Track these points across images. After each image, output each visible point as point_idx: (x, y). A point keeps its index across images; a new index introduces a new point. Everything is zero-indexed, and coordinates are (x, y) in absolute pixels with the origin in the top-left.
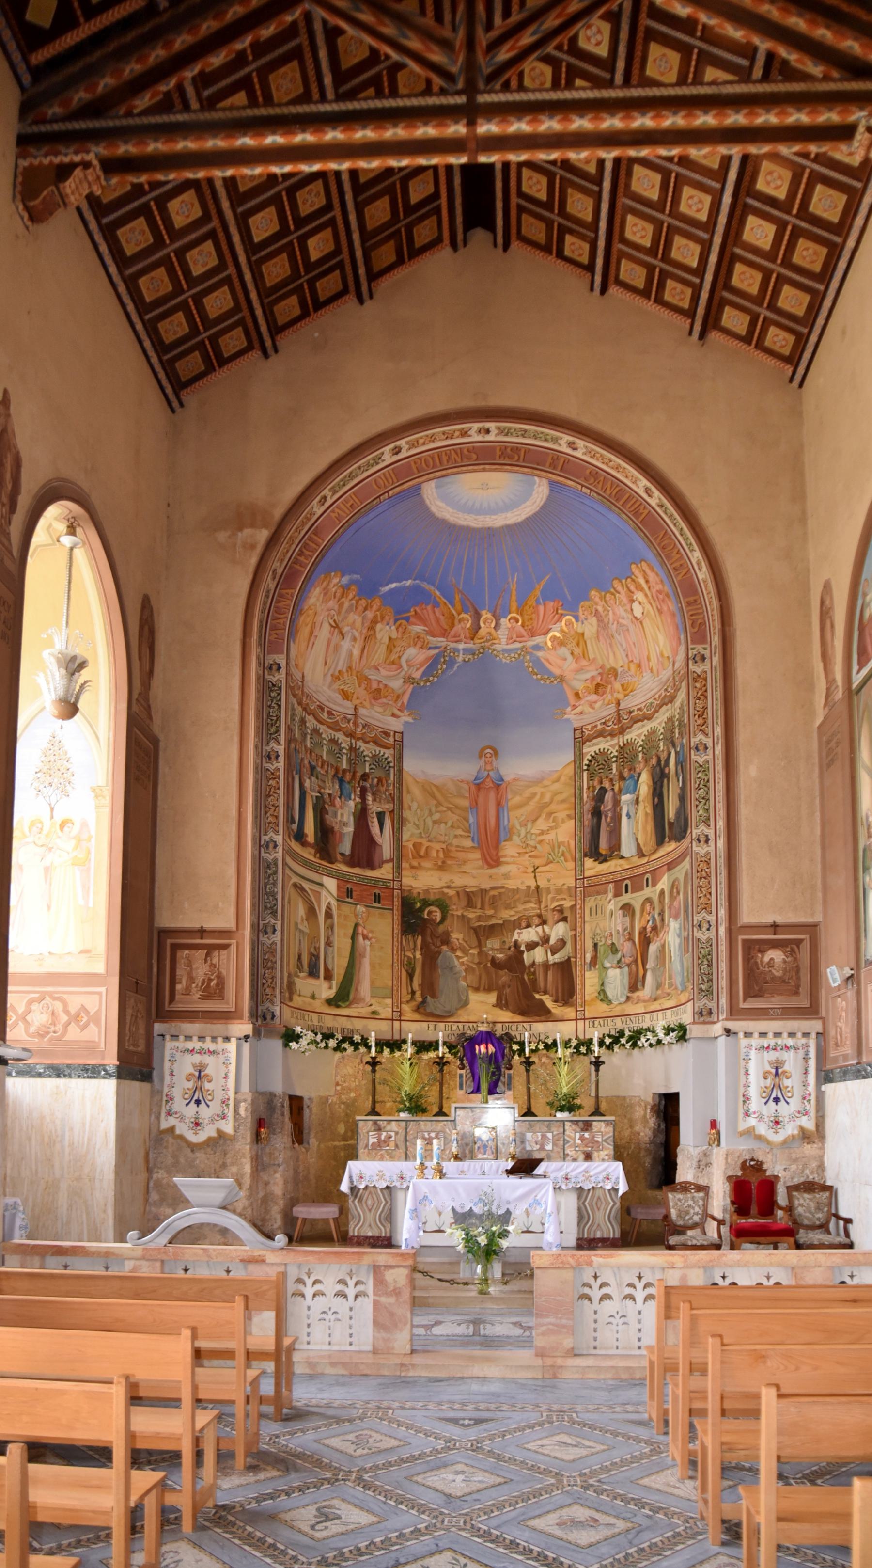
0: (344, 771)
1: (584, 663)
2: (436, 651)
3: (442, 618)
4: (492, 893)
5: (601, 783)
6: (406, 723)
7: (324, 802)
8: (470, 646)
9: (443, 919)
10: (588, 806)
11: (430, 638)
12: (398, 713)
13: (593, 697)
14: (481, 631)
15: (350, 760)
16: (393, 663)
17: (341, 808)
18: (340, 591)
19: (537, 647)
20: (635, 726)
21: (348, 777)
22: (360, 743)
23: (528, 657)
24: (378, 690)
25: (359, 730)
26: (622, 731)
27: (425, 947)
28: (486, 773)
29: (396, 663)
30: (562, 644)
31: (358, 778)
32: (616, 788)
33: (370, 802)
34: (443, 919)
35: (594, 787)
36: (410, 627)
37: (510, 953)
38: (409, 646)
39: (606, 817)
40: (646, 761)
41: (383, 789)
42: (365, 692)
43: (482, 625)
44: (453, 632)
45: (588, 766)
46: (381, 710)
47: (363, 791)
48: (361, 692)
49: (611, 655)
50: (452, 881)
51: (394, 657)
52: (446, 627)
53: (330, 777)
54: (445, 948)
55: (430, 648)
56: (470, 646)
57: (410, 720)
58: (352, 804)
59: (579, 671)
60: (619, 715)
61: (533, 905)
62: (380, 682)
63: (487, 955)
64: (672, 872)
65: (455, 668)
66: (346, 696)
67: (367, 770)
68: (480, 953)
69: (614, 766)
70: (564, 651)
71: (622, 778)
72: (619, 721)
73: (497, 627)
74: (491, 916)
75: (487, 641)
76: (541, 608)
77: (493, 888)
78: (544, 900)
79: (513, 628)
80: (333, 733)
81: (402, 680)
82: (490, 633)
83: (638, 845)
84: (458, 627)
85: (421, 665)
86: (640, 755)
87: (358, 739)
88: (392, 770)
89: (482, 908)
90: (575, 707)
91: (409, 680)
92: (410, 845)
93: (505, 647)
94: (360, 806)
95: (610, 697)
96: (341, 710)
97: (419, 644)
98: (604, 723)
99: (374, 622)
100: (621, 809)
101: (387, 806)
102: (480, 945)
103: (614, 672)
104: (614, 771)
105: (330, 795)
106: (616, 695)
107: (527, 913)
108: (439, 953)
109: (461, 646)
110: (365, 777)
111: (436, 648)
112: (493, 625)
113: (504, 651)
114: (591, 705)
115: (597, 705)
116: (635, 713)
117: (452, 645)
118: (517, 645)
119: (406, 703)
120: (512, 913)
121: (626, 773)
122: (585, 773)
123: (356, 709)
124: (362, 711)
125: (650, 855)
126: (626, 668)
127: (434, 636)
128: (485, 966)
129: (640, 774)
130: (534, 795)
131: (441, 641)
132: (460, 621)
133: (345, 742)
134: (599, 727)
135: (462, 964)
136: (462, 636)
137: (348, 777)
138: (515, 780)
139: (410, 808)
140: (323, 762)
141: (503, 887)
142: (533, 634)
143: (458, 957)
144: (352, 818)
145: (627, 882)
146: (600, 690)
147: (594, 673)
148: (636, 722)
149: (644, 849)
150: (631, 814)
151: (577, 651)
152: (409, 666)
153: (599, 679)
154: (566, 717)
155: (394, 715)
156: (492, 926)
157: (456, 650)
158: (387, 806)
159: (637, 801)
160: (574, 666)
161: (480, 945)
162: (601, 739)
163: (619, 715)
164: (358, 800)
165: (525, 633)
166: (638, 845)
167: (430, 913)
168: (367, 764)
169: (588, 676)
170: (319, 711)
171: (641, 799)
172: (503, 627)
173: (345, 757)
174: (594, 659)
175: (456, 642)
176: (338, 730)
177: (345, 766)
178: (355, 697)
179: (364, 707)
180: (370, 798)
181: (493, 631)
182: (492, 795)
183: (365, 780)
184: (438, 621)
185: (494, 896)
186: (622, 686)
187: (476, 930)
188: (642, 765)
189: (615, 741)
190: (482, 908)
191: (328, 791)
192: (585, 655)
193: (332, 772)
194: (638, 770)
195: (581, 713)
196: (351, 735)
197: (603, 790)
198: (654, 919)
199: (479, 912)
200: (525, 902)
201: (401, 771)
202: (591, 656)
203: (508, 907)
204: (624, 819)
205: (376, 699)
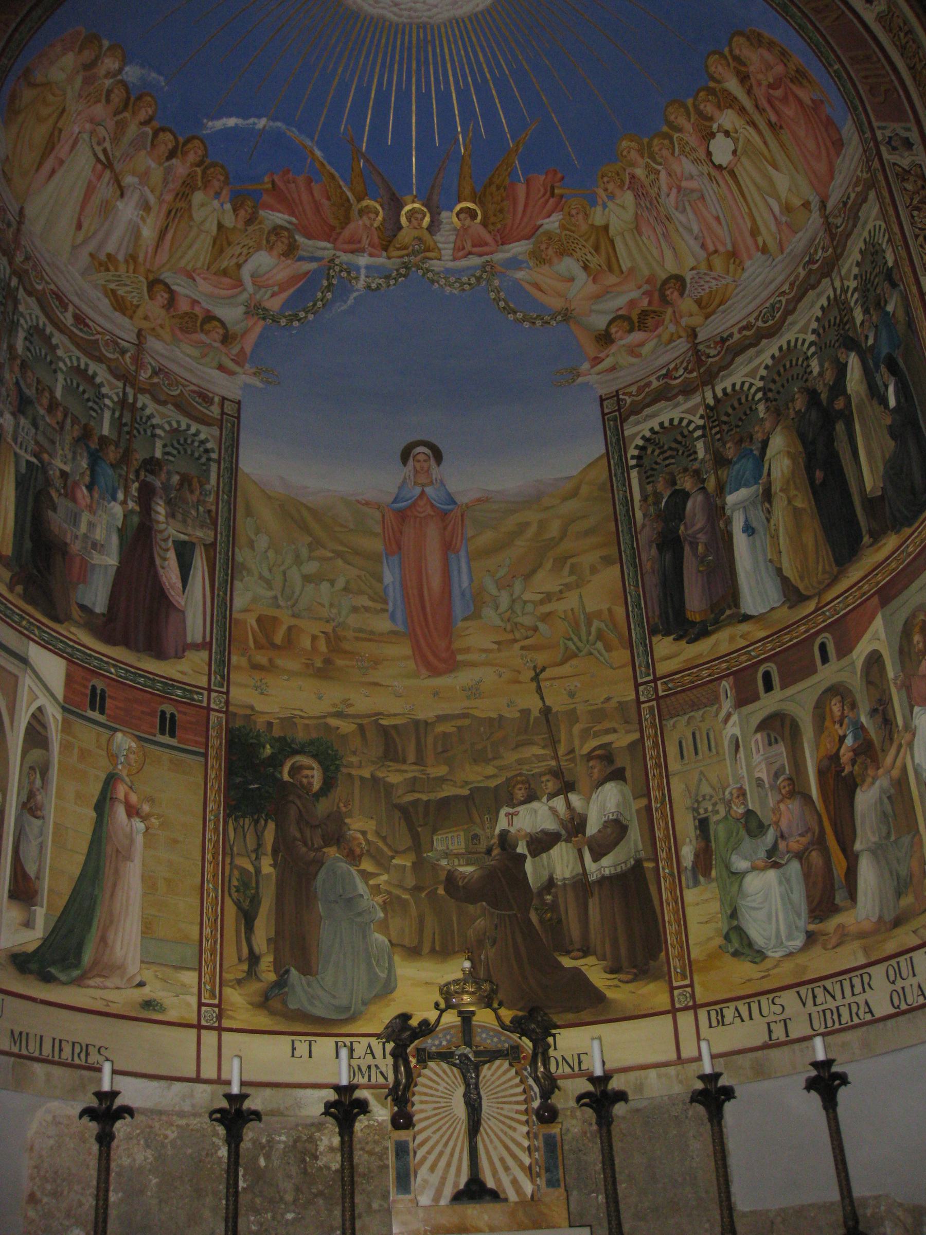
0: (103, 440)
1: (612, 279)
2: (313, 266)
3: (324, 201)
4: (440, 728)
5: (674, 483)
6: (246, 386)
7: (48, 482)
8: (381, 260)
9: (328, 784)
10: (643, 538)
11: (300, 239)
12: (231, 365)
13: (637, 336)
14: (403, 233)
15: (118, 424)
16: (225, 273)
17: (91, 509)
18: (117, 97)
19: (515, 263)
20: (738, 360)
21: (112, 454)
22: (143, 399)
23: (496, 283)
24: (192, 316)
25: (144, 375)
26: (709, 378)
27: (283, 848)
28: (418, 490)
29: (232, 275)
30: (564, 252)
31: (135, 464)
32: (711, 485)
33: (162, 518)
34: (328, 784)
35: (658, 496)
36: (262, 213)
37: (490, 862)
38: (259, 248)
39: (694, 545)
40: (777, 414)
41: (192, 498)
42: (163, 312)
43: (403, 220)
44: (346, 233)
45: (639, 458)
46: (195, 353)
47: (146, 495)
48: (154, 308)
49: (668, 254)
50: (347, 702)
51: (226, 262)
52: (333, 222)
53: (68, 439)
54: (332, 852)
55: (301, 259)
56: (381, 260)
57: (256, 382)
58: (117, 510)
59: (598, 297)
60: (697, 353)
61: (537, 750)
62: (195, 302)
63: (435, 867)
64: (895, 604)
65: (351, 301)
66: (120, 305)
67: (158, 454)
68: (418, 865)
69: (700, 446)
70: (570, 265)
71: (720, 461)
72: (700, 363)
73: (433, 228)
74: (442, 780)
75: (415, 253)
76: (521, 190)
77: (441, 719)
78: (563, 736)
79: (465, 229)
80: (84, 360)
81: (241, 309)
82: (419, 239)
83: (785, 581)
84: (357, 225)
85: (283, 287)
86: (761, 408)
87: (143, 391)
88: (214, 467)
89: (420, 761)
90: (597, 361)
91: (255, 310)
92: (252, 621)
93: (450, 265)
94: (136, 519)
95: (672, 328)
96: (109, 326)
97: (281, 247)
98: (665, 376)
99: (187, 188)
100: (729, 522)
101: (199, 533)
102: (417, 846)
103: (679, 281)
104: (701, 454)
105: (64, 474)
106: (684, 321)
107: (525, 769)
108: (320, 863)
109: (363, 260)
110: (152, 465)
111: (312, 259)
112: (427, 219)
113: (447, 270)
114: (633, 351)
115: (646, 350)
116: (737, 336)
117: (344, 257)
118: (475, 261)
119: (248, 349)
120: (490, 770)
121: (730, 451)
122: (634, 474)
123: (139, 334)
124: (153, 344)
125: (820, 594)
126: (703, 268)
127: (309, 236)
128: (433, 894)
129: (765, 444)
130: (523, 527)
131: (324, 249)
132: (361, 212)
133: (112, 389)
134: (655, 384)
135: (376, 890)
136: (365, 242)
137: (112, 454)
138: (479, 500)
139: (251, 545)
140: (52, 406)
141: (465, 716)
142: (504, 239)
143: (365, 875)
144: (115, 540)
145: (762, 670)
146: (650, 322)
147: (635, 294)
148: (737, 354)
149: (801, 587)
150: (755, 524)
151: (595, 261)
152: (258, 286)
153: (645, 302)
154: (580, 380)
155: (221, 368)
156: (445, 803)
157: (350, 269)
158: (199, 533)
159: (768, 495)
160: (591, 288)
161: (417, 846)
162: (663, 404)
163: (697, 353)
164: (131, 505)
165: (488, 238)
166: (785, 581)
167: (295, 770)
168: (159, 444)
169: (621, 301)
170: (54, 303)
171: (776, 487)
172: (445, 227)
173: (107, 415)
174: (632, 270)
175: (353, 252)
176: (100, 359)
177: (106, 431)
178: (140, 313)
179: (158, 337)
180: (160, 510)
181: (426, 236)
182: (433, 534)
183: (152, 472)
184: (317, 206)
185: (445, 735)
186: (699, 302)
187: (406, 812)
188: (768, 425)
189: (696, 399)
190: (420, 761)
191: (58, 463)
192: (612, 265)
193: (72, 432)
194: (759, 436)
195: (613, 369)
196: (127, 378)
197: (680, 497)
198: (859, 728)
199: (412, 771)
200: (517, 746)
201: (233, 471)
202: (626, 264)
203: (479, 758)
204: (740, 541)
205: (185, 330)
